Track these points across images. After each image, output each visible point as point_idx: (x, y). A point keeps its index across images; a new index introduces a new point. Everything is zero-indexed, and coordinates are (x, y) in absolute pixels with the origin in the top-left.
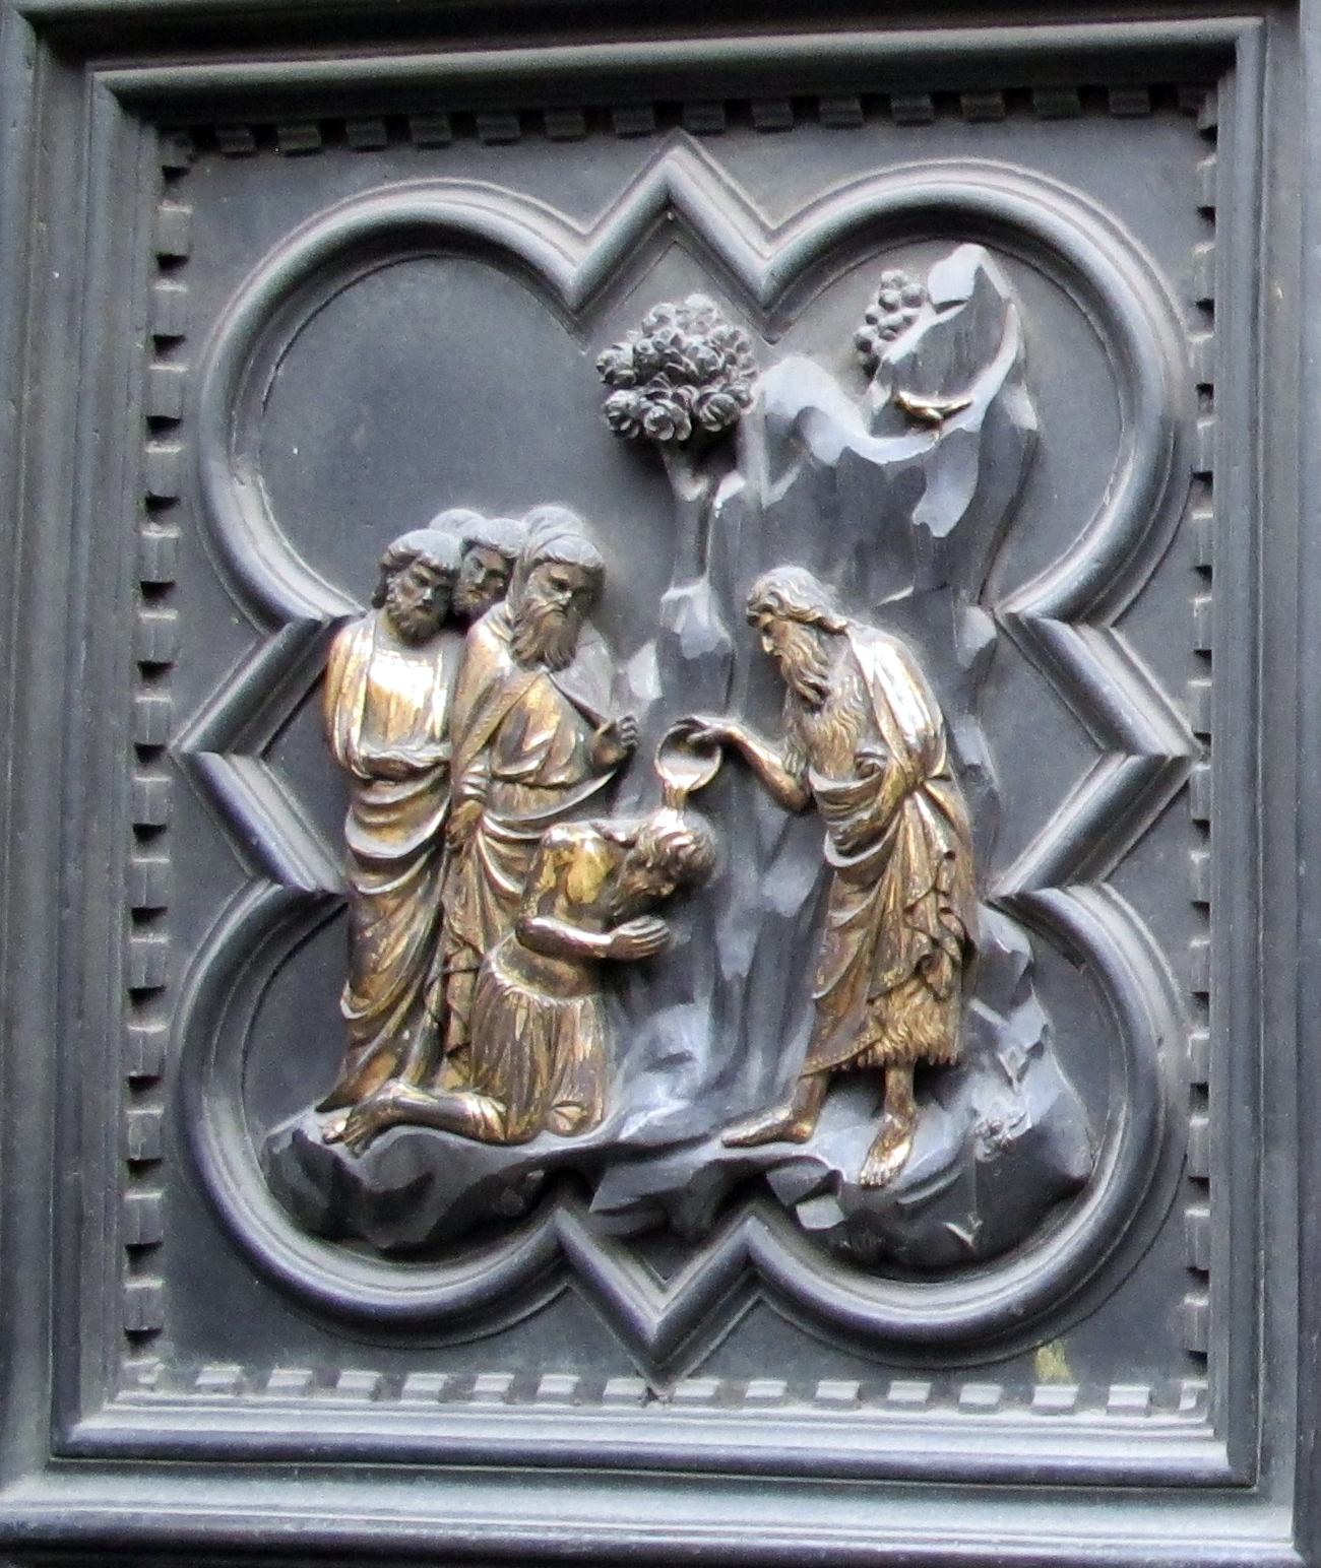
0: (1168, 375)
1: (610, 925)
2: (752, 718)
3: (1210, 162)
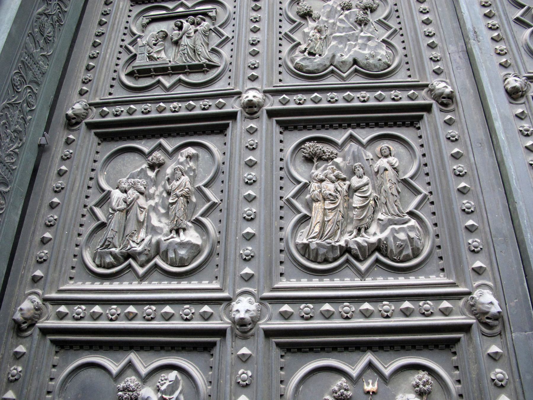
0: (204, 393)
3: (212, 359)
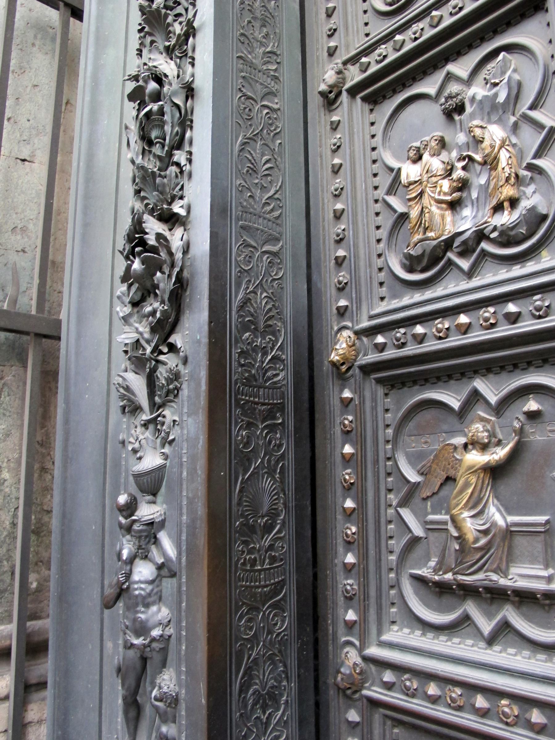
1: (451, 195)
2: (473, 152)
